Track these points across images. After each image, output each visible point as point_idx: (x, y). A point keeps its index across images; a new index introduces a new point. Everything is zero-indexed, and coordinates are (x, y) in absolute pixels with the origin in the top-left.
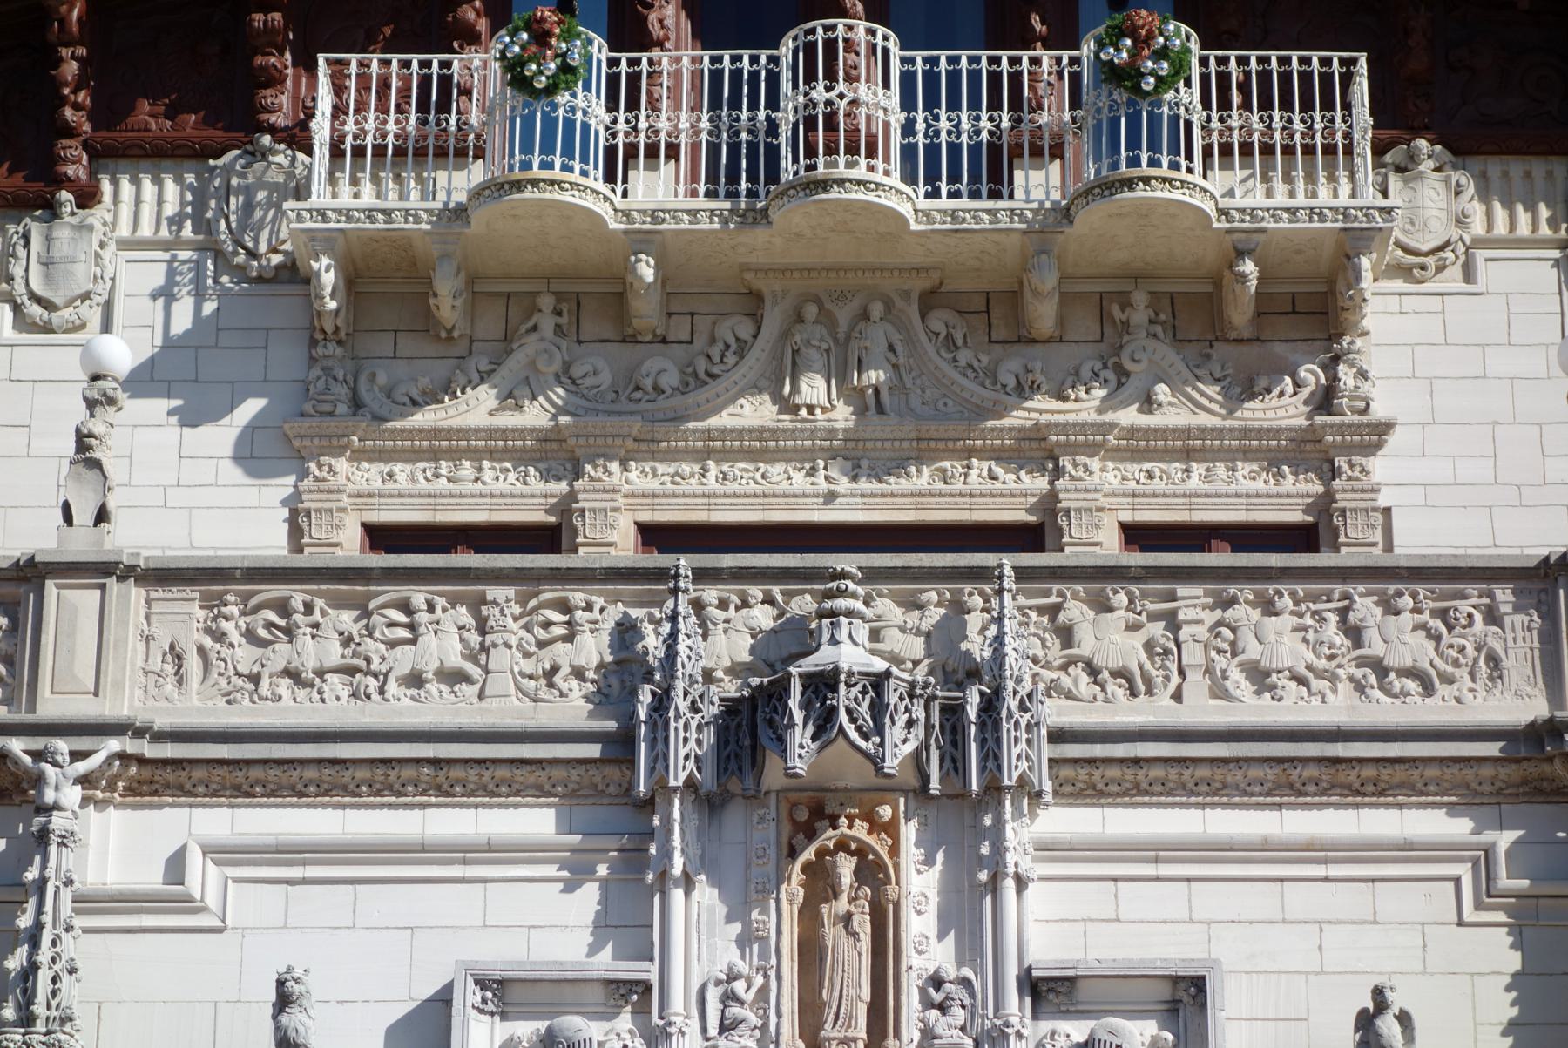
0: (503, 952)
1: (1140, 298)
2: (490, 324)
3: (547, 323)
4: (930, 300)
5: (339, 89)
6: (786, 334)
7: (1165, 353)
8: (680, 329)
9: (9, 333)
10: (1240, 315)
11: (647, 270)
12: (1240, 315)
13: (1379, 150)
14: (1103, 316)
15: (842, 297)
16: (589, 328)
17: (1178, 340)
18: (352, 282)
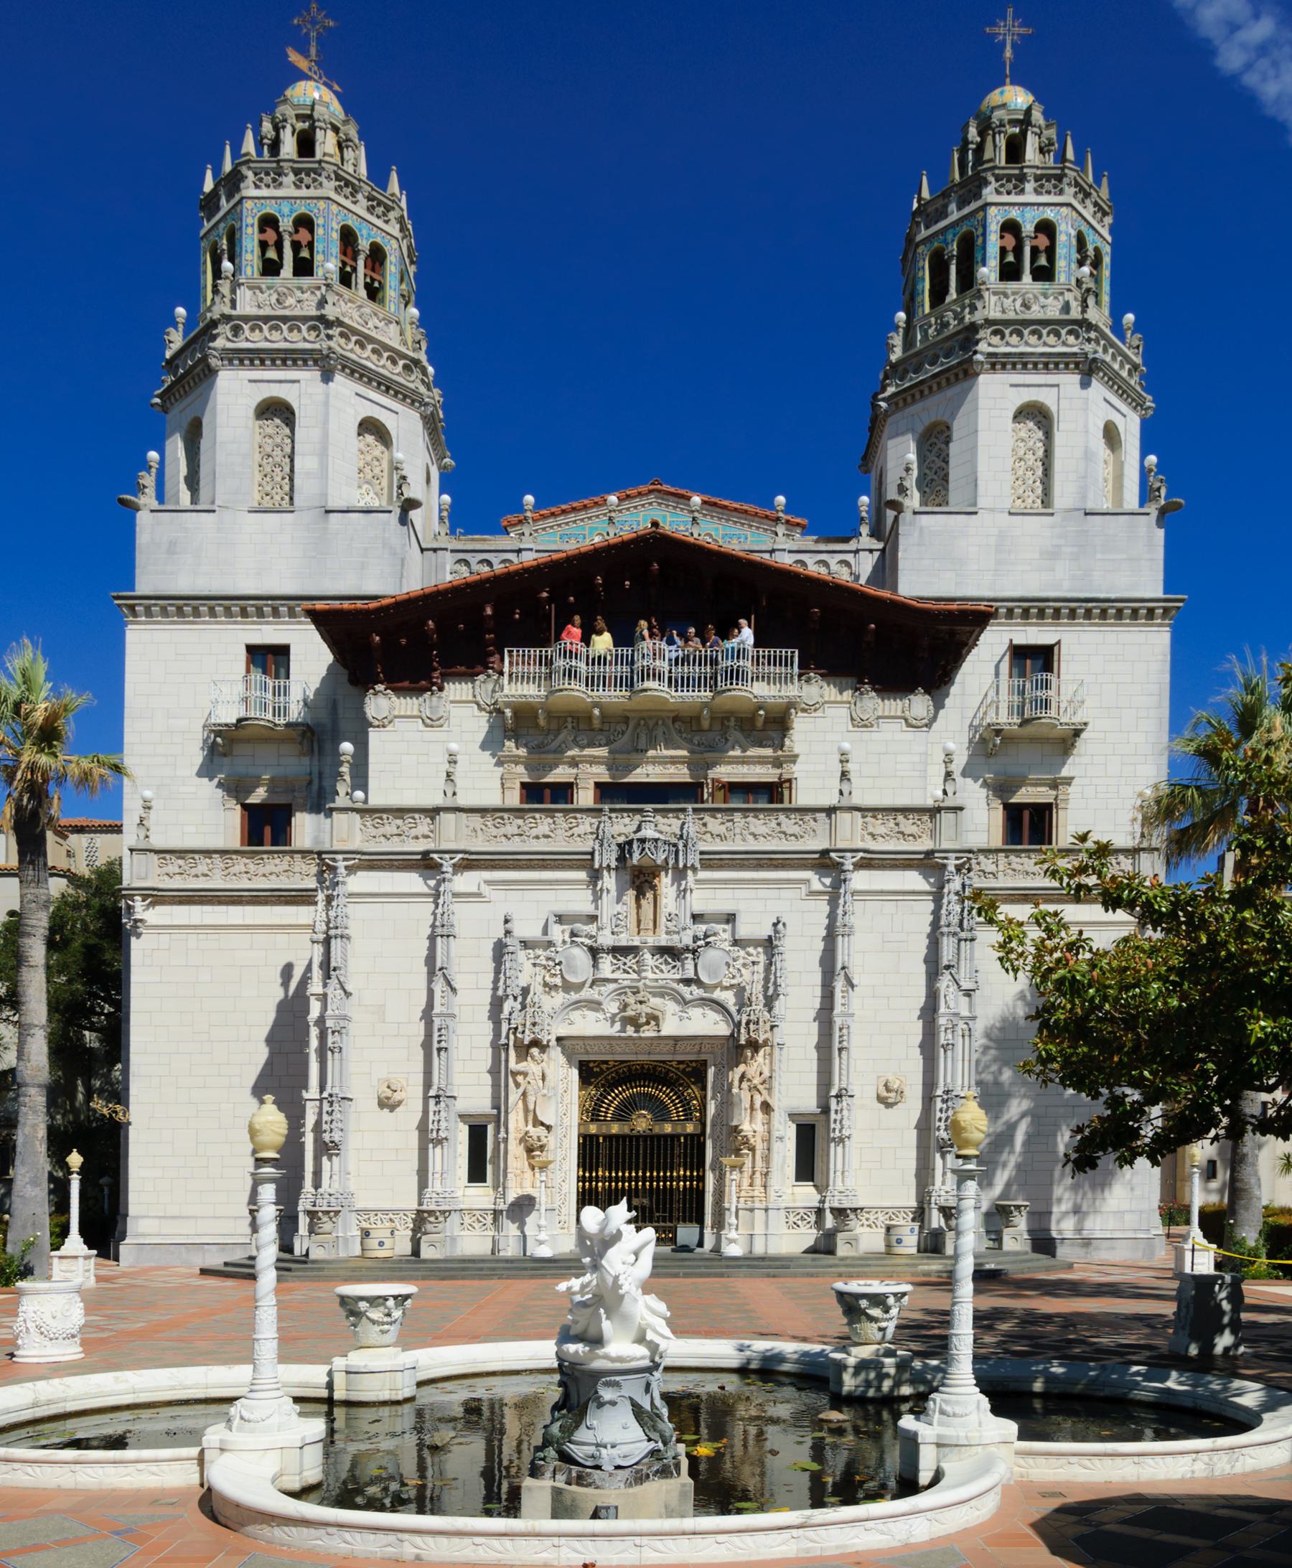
0: (561, 908)
1: (733, 719)
2: (554, 726)
3: (570, 726)
4: (675, 719)
5: (511, 656)
6: (635, 728)
7: (738, 735)
8: (606, 727)
9: (421, 727)
10: (760, 723)
11: (596, 712)
12: (760, 723)
13: (800, 676)
14: (722, 724)
15: (650, 718)
16: (581, 727)
17: (742, 730)
18: (516, 713)
